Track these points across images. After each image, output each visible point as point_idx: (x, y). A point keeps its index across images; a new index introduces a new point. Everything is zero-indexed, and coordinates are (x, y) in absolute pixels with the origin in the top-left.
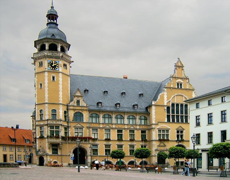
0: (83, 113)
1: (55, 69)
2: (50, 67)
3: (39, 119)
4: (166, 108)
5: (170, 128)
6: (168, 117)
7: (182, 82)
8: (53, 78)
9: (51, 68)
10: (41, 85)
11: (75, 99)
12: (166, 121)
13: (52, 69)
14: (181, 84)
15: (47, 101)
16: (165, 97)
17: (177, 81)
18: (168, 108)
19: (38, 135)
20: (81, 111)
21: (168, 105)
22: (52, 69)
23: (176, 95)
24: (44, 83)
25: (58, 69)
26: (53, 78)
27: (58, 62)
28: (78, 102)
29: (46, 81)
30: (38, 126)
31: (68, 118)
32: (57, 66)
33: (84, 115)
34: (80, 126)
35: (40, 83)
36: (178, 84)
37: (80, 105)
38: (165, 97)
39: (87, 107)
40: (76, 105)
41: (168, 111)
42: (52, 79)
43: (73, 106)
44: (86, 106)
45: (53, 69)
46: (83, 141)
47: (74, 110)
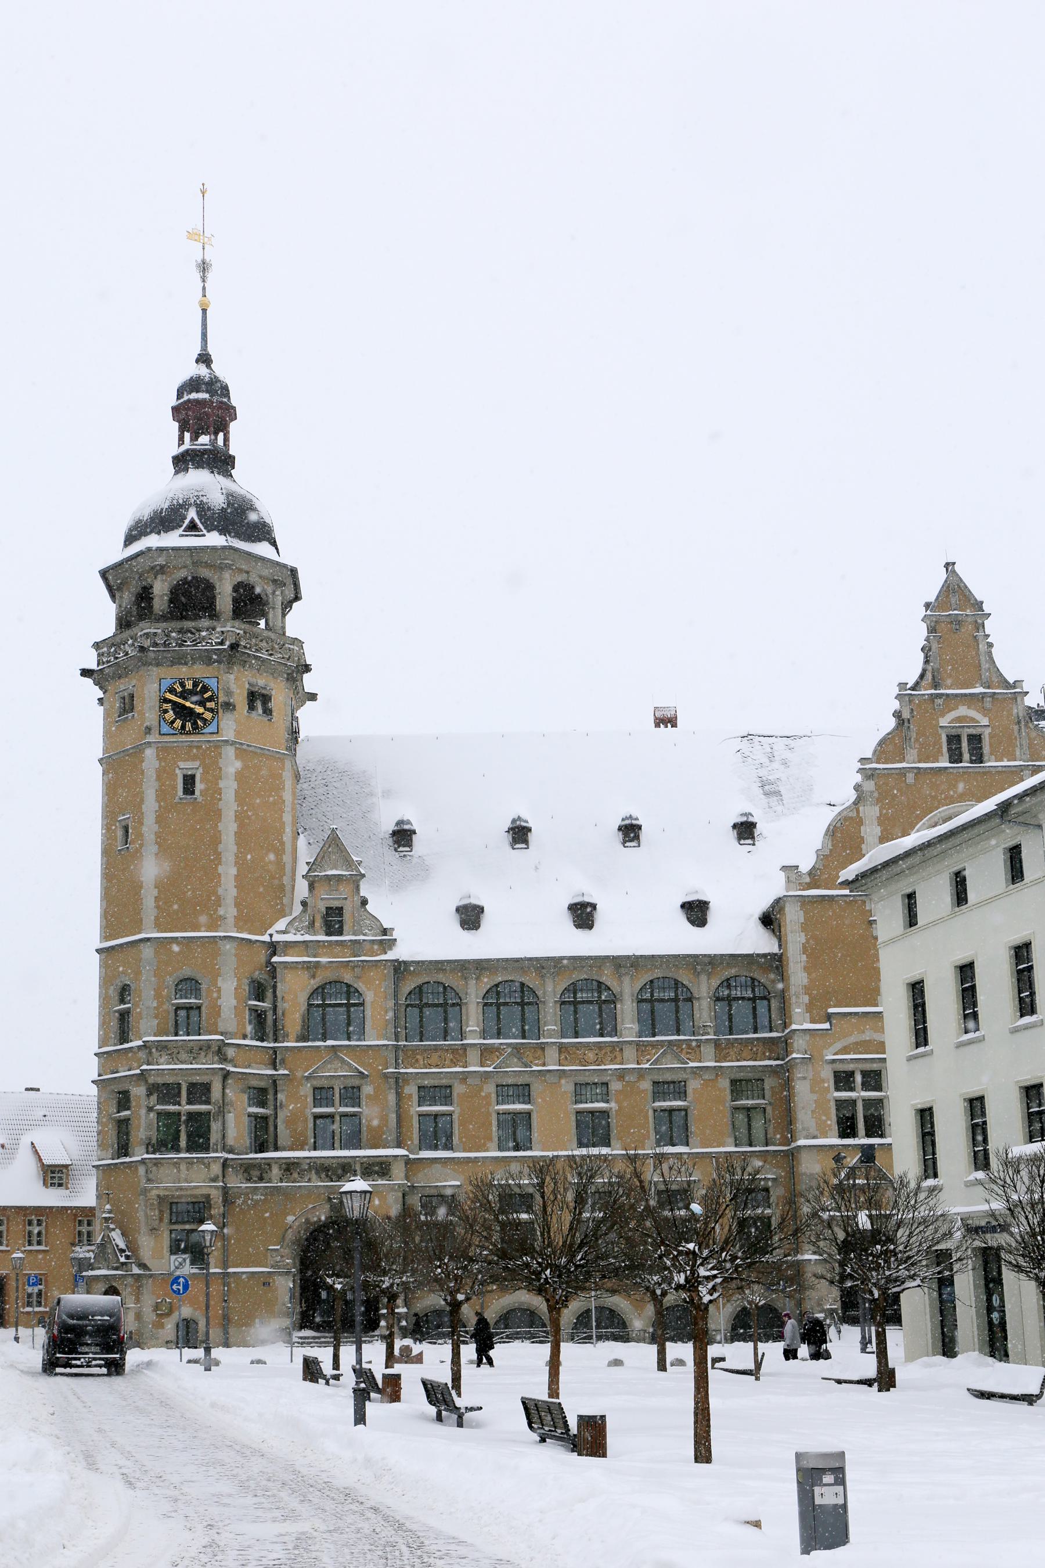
0: (361, 986)
1: (195, 726)
2: (170, 716)
9: (178, 723)
13: (183, 727)
20: (348, 977)
27: (212, 683)
29: (150, 805)
33: (369, 997)
45: (189, 725)
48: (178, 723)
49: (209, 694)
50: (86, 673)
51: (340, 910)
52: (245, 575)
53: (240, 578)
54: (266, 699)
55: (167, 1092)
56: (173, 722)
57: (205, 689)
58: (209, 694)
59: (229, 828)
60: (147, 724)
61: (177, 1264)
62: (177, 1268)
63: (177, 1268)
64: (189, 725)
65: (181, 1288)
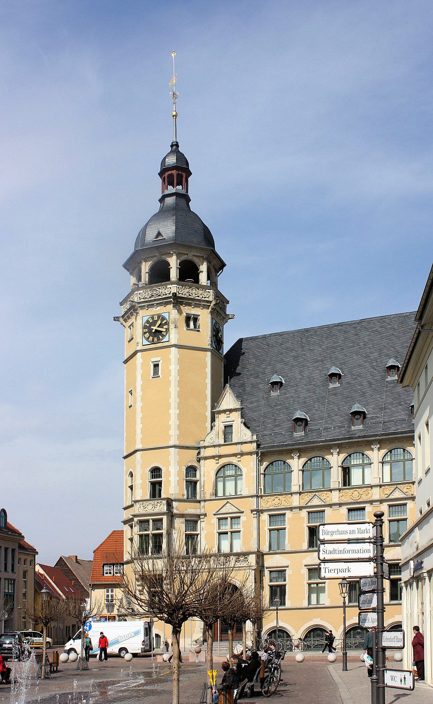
0: (240, 465)
2: (147, 335)
8: (156, 366)
13: (153, 340)
15: (139, 446)
20: (234, 460)
22: (153, 343)
24: (135, 390)
26: (156, 366)
27: (166, 315)
28: (228, 428)
29: (139, 383)
33: (244, 471)
40: (222, 442)
42: (152, 374)
44: (250, 440)
45: (156, 339)
48: (151, 338)
49: (165, 321)
50: (116, 319)
51: (232, 425)
52: (186, 256)
53: (184, 257)
54: (195, 320)
55: (143, 523)
57: (163, 318)
58: (165, 321)
60: (137, 341)
64: (156, 339)
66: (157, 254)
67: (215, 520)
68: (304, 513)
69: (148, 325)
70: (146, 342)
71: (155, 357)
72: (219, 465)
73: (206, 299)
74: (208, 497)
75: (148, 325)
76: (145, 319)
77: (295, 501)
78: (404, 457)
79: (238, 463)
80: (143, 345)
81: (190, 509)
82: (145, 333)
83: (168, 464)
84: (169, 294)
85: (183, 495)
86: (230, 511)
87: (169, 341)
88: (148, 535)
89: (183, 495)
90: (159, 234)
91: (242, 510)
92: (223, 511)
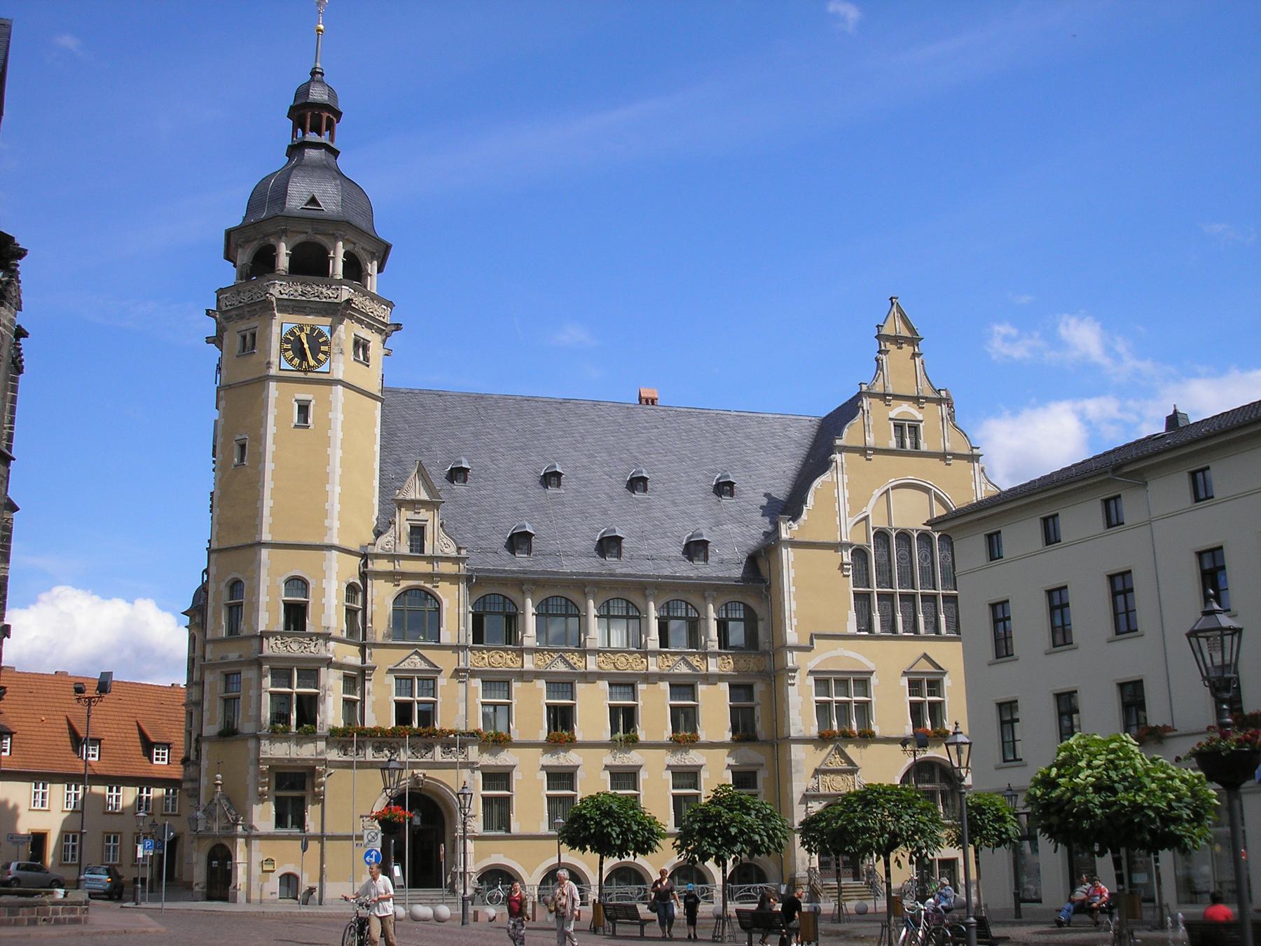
0: (438, 592)
2: (290, 354)
3: (224, 633)
4: (847, 557)
5: (870, 666)
6: (862, 600)
7: (920, 417)
8: (304, 409)
10: (243, 447)
11: (404, 519)
12: (852, 628)
14: (915, 429)
16: (844, 494)
17: (892, 414)
18: (860, 554)
19: (211, 722)
21: (860, 540)
23: (893, 488)
25: (325, 368)
26: (304, 409)
28: (418, 532)
30: (213, 666)
31: (364, 622)
32: (325, 353)
33: (446, 604)
34: (424, 666)
35: (238, 437)
36: (899, 427)
37: (428, 551)
38: (844, 494)
39: (456, 560)
41: (862, 577)
43: (393, 557)
44: (454, 554)
46: (438, 749)
47: (393, 576)
49: (324, 339)
56: (292, 360)
58: (324, 339)
59: (336, 454)
61: (370, 837)
62: (370, 841)
63: (370, 841)
65: (373, 860)
66: (309, 231)
67: (391, 680)
68: (604, 685)
69: (292, 338)
70: (285, 365)
71: (304, 393)
72: (399, 588)
73: (381, 319)
74: (379, 639)
75: (292, 338)
76: (287, 328)
77: (529, 663)
78: (628, 612)
79: (434, 589)
80: (280, 370)
81: (350, 655)
82: (286, 350)
83: (322, 575)
84: (336, 298)
85: (342, 631)
86: (419, 667)
87: (329, 373)
88: (290, 694)
89: (342, 631)
90: (313, 201)
91: (441, 667)
92: (405, 666)
